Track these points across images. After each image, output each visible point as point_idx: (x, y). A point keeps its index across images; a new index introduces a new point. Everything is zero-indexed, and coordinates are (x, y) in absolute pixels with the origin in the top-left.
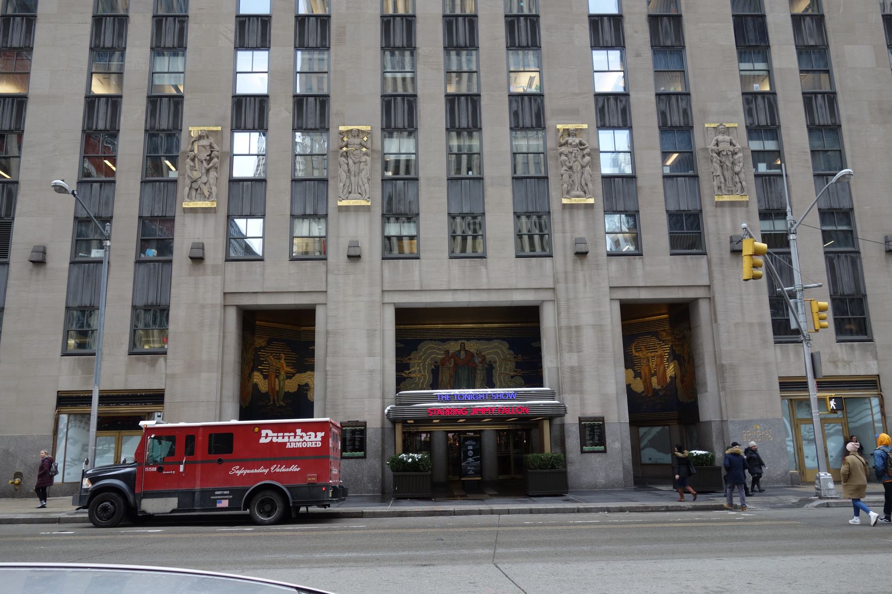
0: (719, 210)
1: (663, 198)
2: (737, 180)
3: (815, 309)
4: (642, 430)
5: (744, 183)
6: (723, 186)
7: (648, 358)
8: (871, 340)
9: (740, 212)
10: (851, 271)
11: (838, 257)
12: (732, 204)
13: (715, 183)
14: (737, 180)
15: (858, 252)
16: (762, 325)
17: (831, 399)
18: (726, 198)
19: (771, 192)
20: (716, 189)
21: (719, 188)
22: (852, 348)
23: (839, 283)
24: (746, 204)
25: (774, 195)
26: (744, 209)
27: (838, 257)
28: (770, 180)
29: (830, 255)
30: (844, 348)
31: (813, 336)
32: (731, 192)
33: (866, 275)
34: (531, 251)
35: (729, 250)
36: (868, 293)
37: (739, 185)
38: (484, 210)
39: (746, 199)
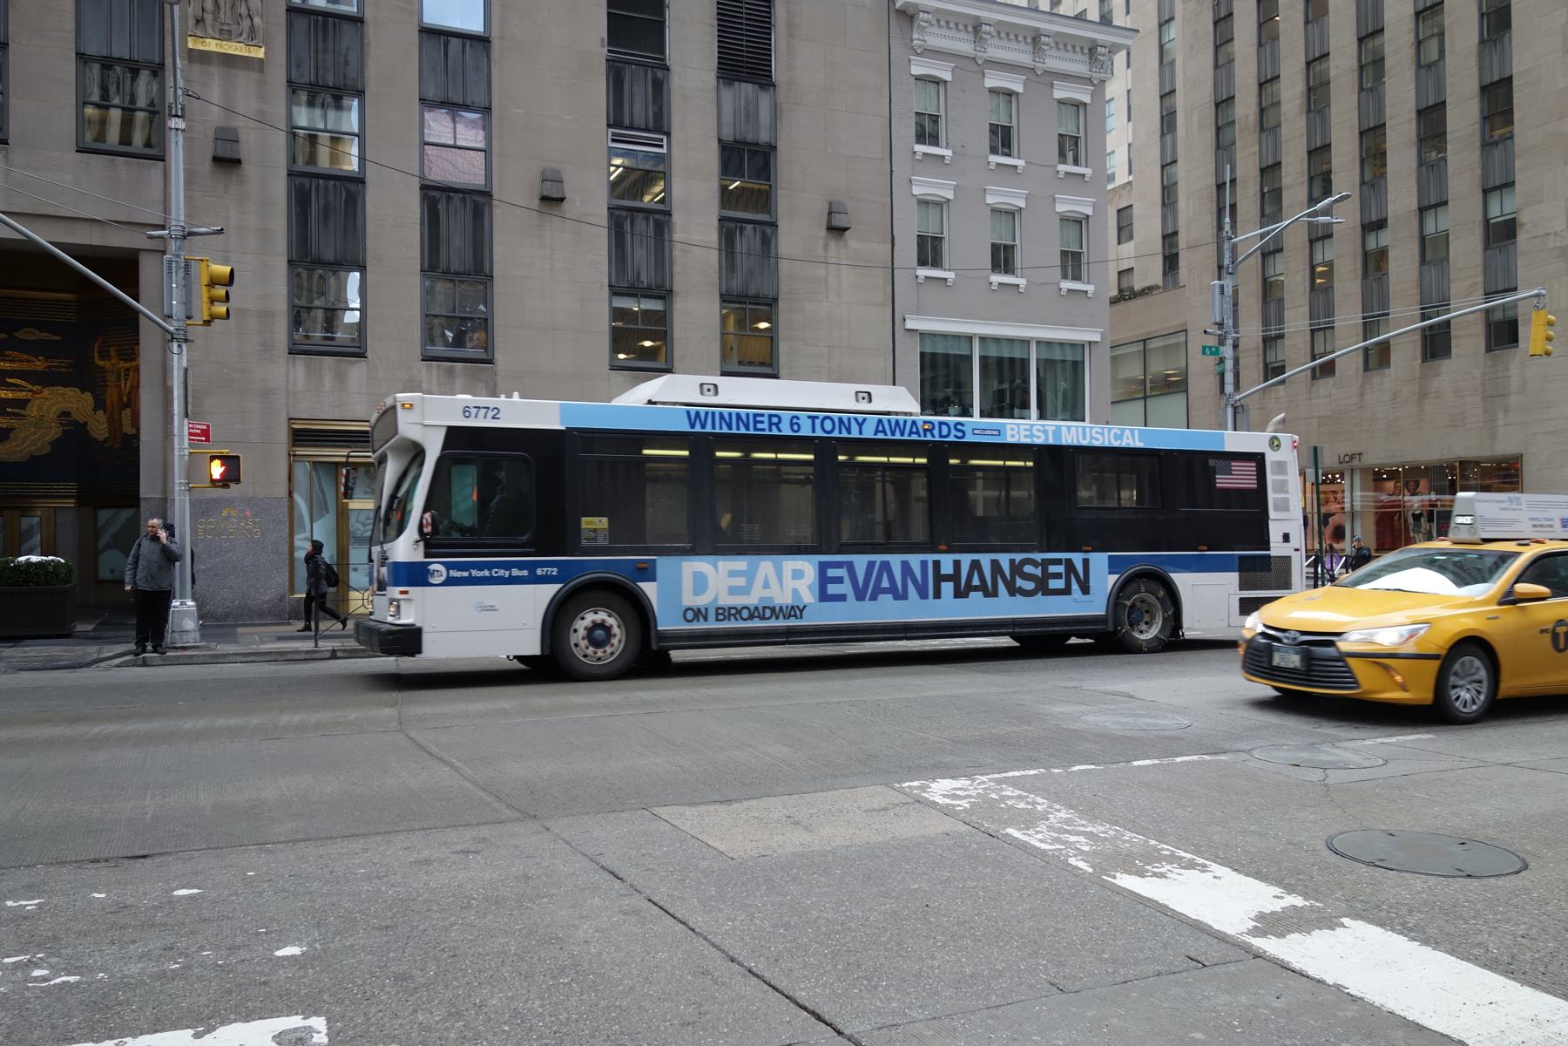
0: (197, 68)
1: (70, 23)
2: (244, 11)
3: (205, 280)
4: (104, 515)
5: (257, 20)
6: (209, 18)
7: (118, 372)
8: (490, 362)
9: (246, 80)
10: (469, 228)
11: (449, 199)
12: (228, 60)
13: (190, 10)
14: (244, 11)
15: (774, 225)
16: (266, 315)
17: (213, 458)
18: (212, 45)
19: (325, 50)
20: (191, 22)
21: (199, 21)
22: (450, 372)
23: (443, 249)
24: (259, 65)
25: (330, 57)
26: (253, 76)
27: (449, 199)
28: (325, 24)
29: (432, 193)
30: (435, 372)
31: (197, 332)
32: (225, 35)
33: (496, 238)
34: (121, 143)
35: (209, 157)
36: (495, 274)
37: (247, 22)
38: (6, 37)
39: (260, 53)
